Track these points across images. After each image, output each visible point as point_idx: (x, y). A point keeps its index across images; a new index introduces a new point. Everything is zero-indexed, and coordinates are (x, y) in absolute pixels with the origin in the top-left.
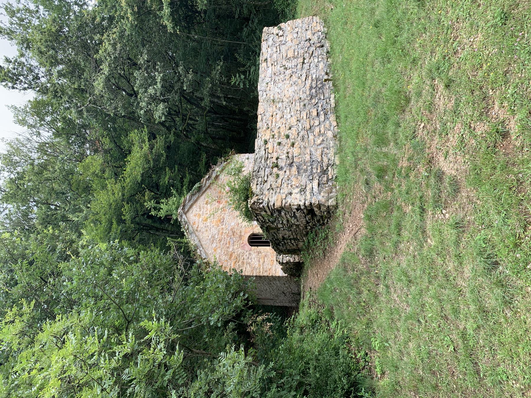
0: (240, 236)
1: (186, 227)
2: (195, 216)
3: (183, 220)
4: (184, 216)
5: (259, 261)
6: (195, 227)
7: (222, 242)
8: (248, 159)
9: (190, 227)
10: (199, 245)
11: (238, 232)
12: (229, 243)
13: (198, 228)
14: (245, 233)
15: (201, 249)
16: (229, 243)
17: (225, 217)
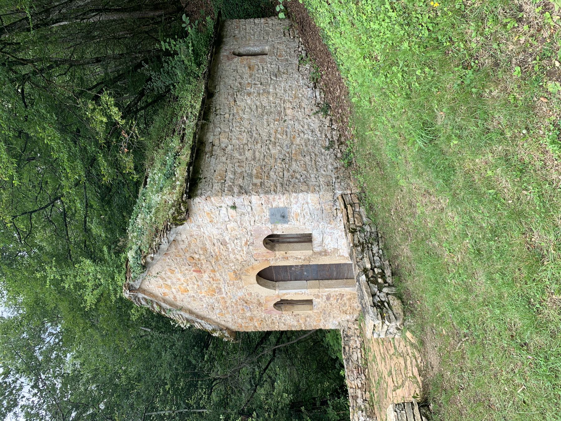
0: (260, 304)
1: (157, 309)
2: (161, 287)
3: (143, 303)
4: (141, 295)
5: (298, 321)
6: (170, 297)
7: (230, 310)
8: (234, 207)
9: (163, 305)
10: (193, 318)
11: (255, 301)
12: (243, 310)
13: (175, 297)
14: (267, 301)
15: (199, 321)
16: (243, 310)
17: (222, 286)
